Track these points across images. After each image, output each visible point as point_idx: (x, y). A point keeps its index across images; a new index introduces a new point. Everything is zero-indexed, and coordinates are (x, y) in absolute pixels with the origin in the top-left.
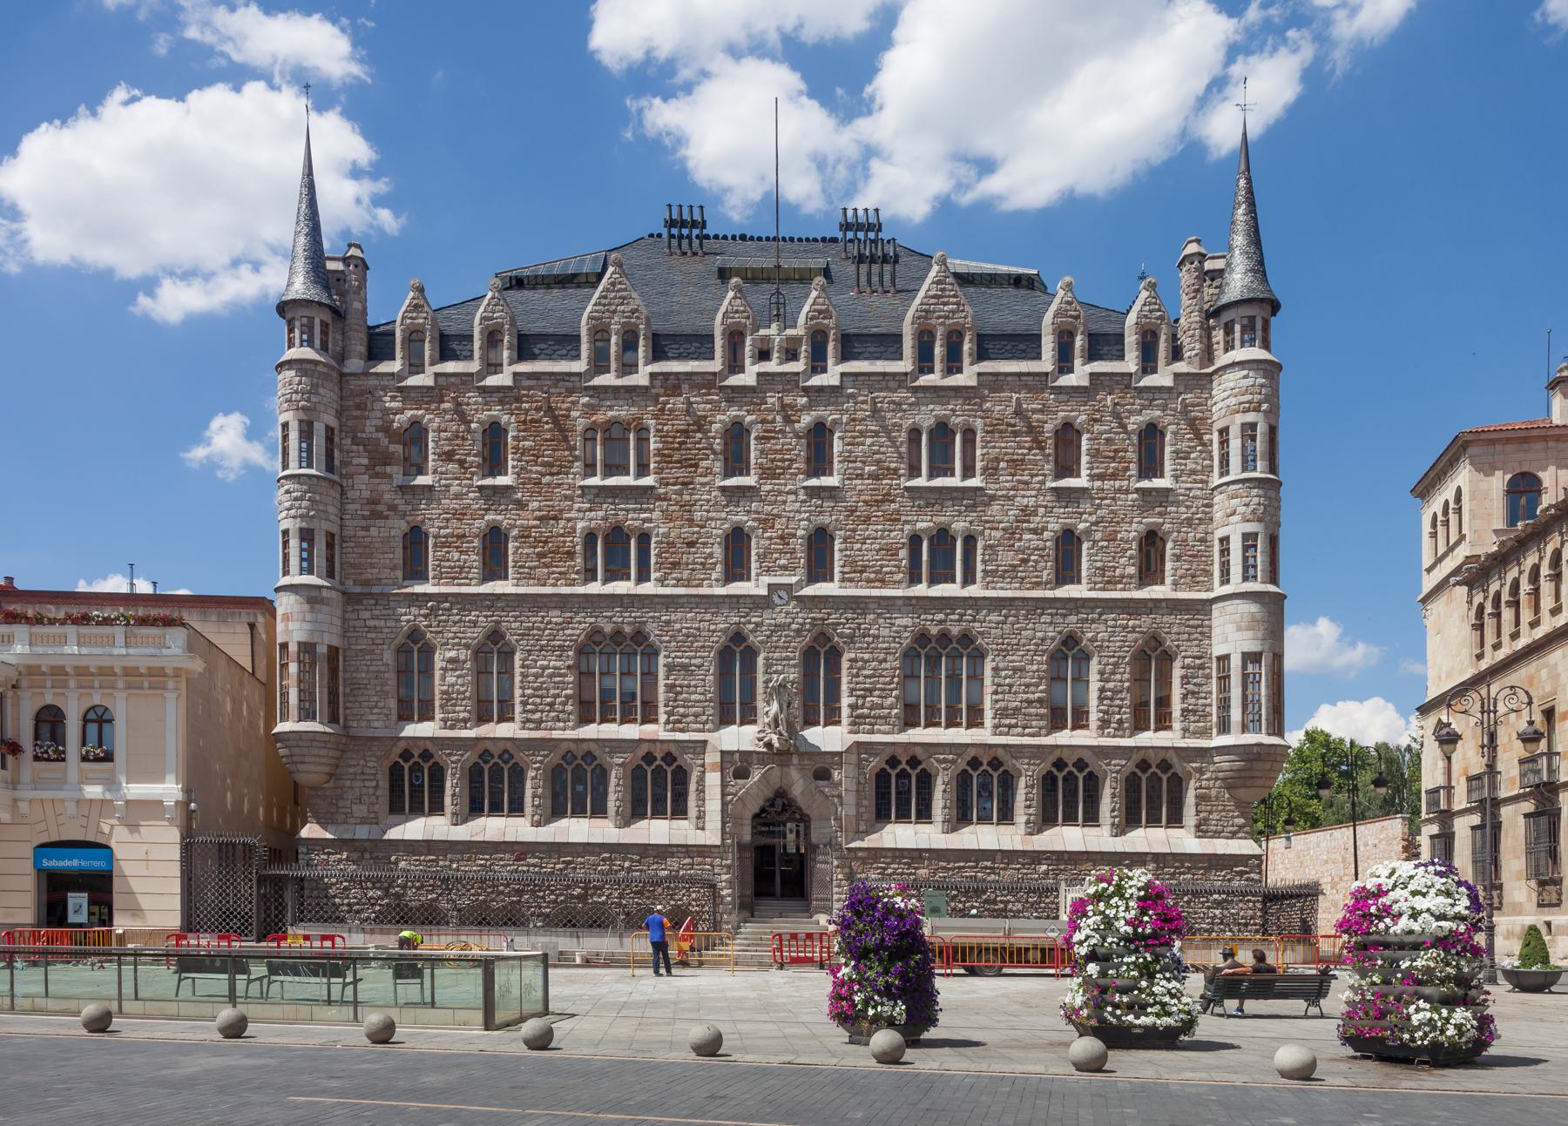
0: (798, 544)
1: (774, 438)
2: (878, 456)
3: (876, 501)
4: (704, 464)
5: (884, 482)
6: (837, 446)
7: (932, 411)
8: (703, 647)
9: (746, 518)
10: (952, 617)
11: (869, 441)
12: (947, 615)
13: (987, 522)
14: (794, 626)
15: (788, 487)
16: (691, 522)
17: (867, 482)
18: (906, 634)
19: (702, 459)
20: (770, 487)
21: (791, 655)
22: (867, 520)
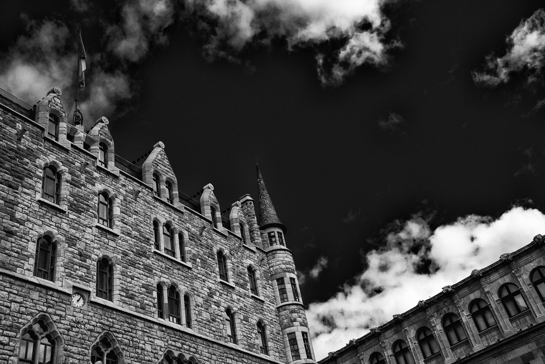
0: (93, 264)
1: (79, 187)
2: (139, 227)
3: (139, 254)
4: (30, 181)
5: (143, 244)
6: (117, 211)
7: (164, 215)
8: (11, 326)
9: (57, 232)
10: (185, 346)
11: (135, 216)
12: (183, 344)
13: (194, 290)
14: (88, 326)
15: (86, 223)
16: (13, 218)
17: (133, 240)
18: (161, 353)
19: (27, 177)
20: (74, 217)
21: (86, 351)
22: (133, 264)
